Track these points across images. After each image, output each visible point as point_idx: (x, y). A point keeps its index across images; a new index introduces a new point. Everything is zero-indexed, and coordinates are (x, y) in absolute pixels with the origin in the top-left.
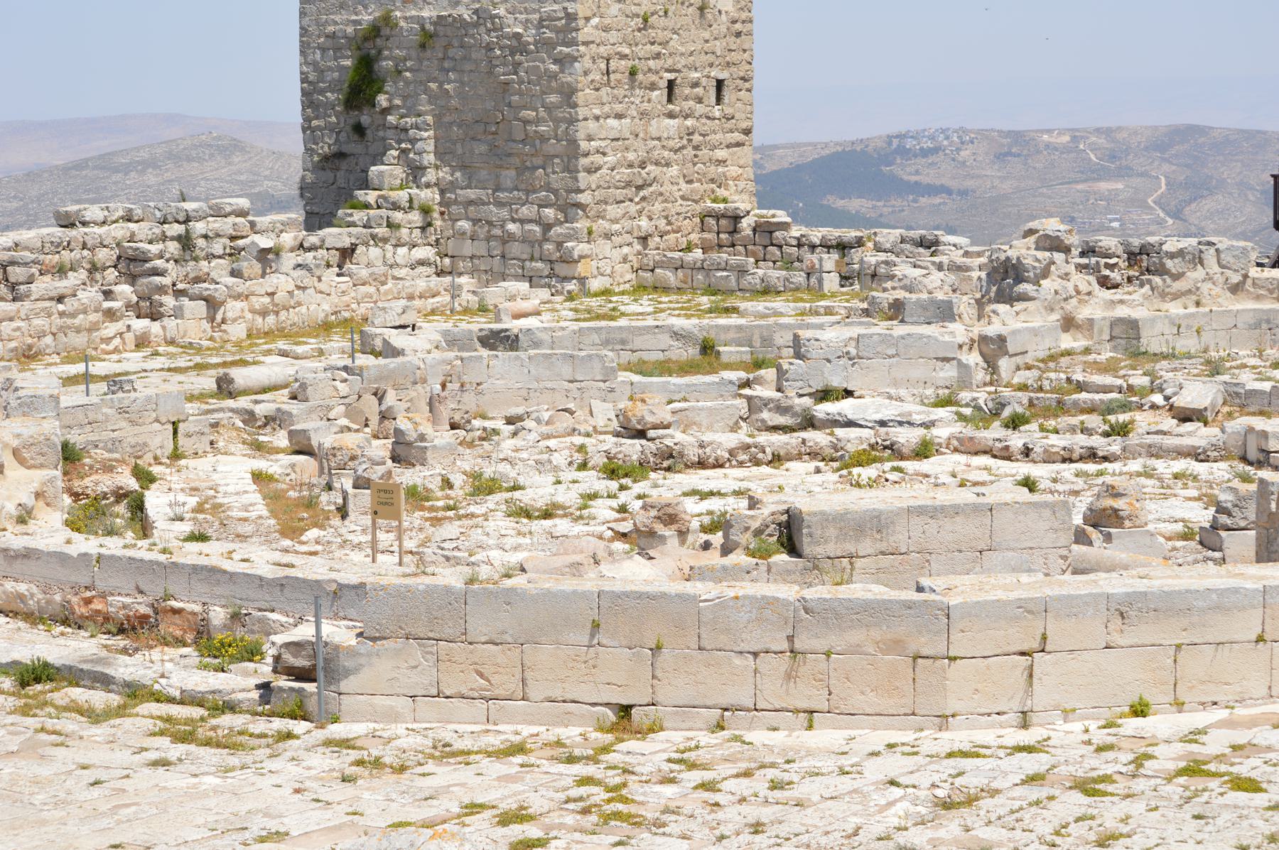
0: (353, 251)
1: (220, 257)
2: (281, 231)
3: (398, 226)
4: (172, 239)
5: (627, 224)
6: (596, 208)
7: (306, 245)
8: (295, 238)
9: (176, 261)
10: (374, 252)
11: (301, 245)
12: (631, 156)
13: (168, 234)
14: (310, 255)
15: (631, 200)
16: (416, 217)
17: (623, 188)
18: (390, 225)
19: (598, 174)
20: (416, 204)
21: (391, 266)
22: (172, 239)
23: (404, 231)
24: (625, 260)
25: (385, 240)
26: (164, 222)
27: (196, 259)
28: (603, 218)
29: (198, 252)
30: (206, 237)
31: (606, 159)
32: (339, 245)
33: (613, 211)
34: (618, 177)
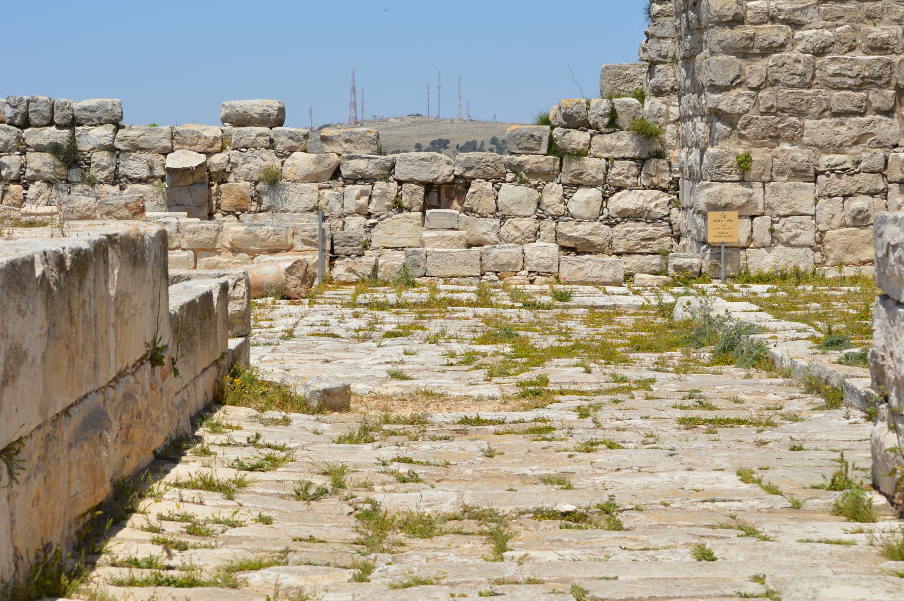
0: (467, 186)
1: (140, 181)
2: (292, 150)
3: (580, 154)
4: (39, 149)
5: (871, 157)
6: (763, 122)
7: (345, 172)
8: (319, 162)
9: (49, 183)
10: (510, 193)
11: (336, 173)
12: (880, 31)
13: (29, 141)
14: (355, 190)
15: (889, 113)
16: (623, 142)
17: (859, 88)
18: (553, 148)
19: (770, 61)
20: (623, 119)
21: (556, 218)
22: (39, 149)
23: (589, 161)
24: (860, 220)
25: (549, 176)
26: (26, 123)
27: (92, 182)
28: (792, 140)
29: (93, 172)
30: (111, 149)
31: (798, 34)
32: (425, 176)
33: (817, 128)
34: (833, 68)
